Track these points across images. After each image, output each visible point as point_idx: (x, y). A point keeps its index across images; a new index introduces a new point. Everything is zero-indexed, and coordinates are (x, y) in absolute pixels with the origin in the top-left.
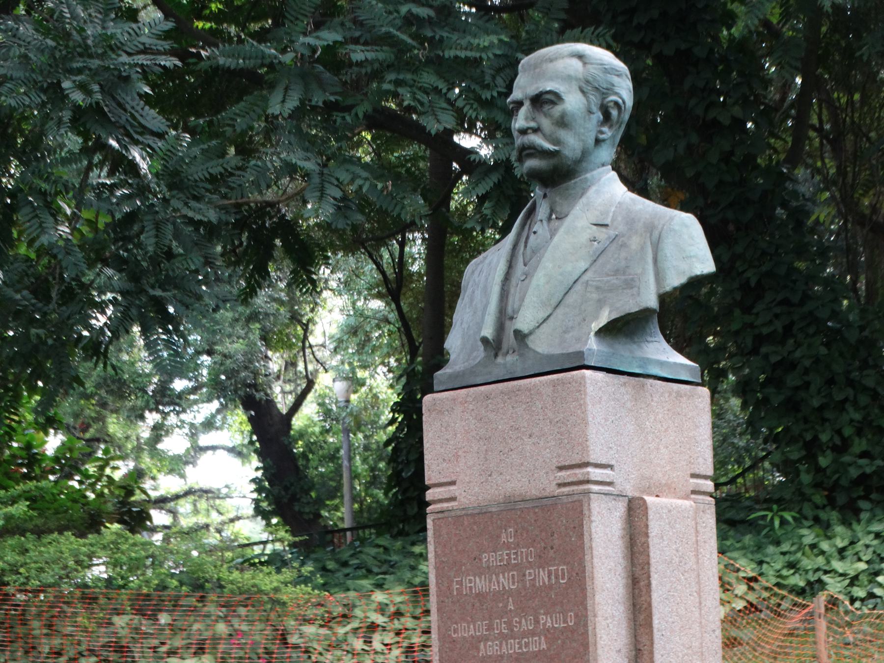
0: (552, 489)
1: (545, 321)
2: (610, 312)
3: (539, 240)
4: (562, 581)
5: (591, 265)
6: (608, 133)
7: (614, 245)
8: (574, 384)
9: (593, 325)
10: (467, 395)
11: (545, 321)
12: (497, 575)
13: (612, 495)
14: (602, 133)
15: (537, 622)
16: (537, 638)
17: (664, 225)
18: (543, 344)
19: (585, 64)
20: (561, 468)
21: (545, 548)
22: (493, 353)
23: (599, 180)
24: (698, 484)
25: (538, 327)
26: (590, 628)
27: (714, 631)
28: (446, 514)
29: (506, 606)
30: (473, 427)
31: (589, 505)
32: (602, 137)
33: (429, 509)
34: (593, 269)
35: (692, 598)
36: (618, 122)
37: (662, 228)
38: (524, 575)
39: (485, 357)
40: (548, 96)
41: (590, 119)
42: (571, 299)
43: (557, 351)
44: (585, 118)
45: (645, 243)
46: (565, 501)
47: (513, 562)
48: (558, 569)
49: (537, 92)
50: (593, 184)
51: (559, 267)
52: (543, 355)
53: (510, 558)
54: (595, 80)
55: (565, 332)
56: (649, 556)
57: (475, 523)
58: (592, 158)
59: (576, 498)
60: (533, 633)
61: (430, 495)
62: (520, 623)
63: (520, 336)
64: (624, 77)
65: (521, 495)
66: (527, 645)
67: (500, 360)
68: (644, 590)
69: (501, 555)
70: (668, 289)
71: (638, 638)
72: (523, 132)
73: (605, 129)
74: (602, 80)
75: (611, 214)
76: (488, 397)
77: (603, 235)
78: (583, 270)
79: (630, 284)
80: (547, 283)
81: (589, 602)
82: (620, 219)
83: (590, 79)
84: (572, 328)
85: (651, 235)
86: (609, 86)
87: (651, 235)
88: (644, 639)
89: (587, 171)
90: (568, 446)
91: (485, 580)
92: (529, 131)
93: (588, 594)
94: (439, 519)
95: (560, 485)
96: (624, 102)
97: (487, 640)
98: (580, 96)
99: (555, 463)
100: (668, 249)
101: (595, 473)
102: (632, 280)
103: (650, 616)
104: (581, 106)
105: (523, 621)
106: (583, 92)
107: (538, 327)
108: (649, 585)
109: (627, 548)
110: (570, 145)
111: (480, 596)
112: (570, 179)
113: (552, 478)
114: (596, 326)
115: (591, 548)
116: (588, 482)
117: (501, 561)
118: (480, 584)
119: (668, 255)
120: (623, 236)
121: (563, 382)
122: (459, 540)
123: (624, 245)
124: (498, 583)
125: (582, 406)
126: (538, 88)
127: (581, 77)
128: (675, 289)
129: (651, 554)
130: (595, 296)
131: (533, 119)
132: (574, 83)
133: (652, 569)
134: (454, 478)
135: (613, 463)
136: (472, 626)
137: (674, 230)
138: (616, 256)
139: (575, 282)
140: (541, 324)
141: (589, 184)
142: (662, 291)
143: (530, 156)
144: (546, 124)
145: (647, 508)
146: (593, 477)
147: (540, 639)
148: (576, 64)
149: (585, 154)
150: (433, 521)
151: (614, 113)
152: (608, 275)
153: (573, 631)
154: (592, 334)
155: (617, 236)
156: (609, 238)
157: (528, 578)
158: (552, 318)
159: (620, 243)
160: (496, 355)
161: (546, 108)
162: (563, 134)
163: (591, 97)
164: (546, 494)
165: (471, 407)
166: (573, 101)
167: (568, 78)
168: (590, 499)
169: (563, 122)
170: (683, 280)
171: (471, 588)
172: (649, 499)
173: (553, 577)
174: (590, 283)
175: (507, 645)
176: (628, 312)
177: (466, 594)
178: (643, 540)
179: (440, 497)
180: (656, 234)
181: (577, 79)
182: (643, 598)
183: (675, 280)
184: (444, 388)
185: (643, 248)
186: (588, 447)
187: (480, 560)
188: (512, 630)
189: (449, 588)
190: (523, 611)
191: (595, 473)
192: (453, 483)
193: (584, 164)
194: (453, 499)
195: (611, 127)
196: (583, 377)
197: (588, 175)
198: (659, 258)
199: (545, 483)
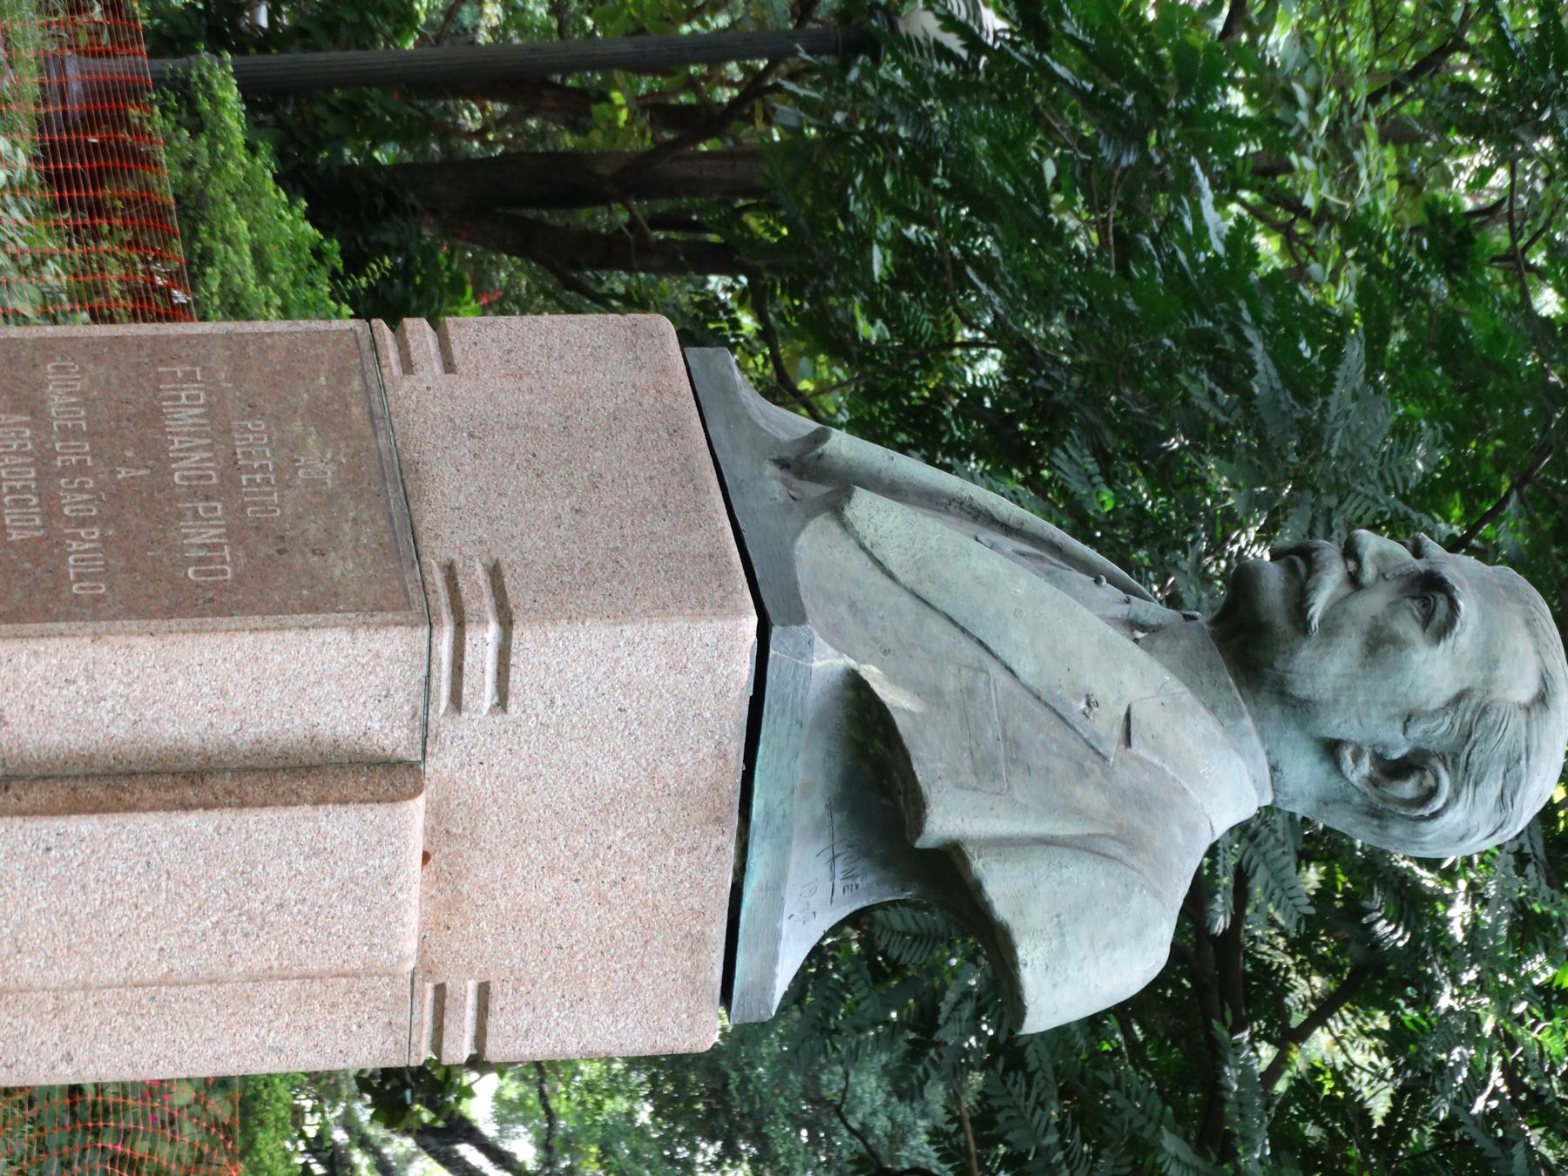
0: (436, 554)
1: (879, 564)
2: (910, 713)
3: (1079, 587)
4: (190, 572)
5: (1025, 686)
6: (1359, 771)
7: (1082, 750)
8: (721, 593)
9: (874, 669)
10: (677, 395)
11: (879, 564)
12: (209, 448)
13: (427, 706)
14: (1356, 757)
15: (82, 523)
16: (38, 522)
17: (1140, 872)
18: (816, 550)
19: (1527, 709)
20: (495, 572)
21: (282, 538)
22: (788, 454)
23: (1237, 751)
24: (463, 1006)
25: (863, 547)
26: (62, 626)
27: (68, 1058)
28: (368, 354)
29: (125, 463)
30: (597, 403)
31: (397, 624)
32: (1347, 755)
33: (380, 324)
34: (1018, 691)
35: (154, 957)
36: (1385, 800)
37: (1133, 868)
38: (207, 498)
39: (778, 442)
40: (1442, 606)
41: (1391, 718)
42: (936, 626)
43: (803, 574)
44: (1393, 703)
45: (1092, 820)
46: (407, 577)
47: (244, 478)
48: (224, 562)
49: (1450, 580)
50: (1228, 731)
51: (1017, 613)
52: (792, 547)
53: (255, 471)
54: (1490, 730)
55: (852, 605)
56: (264, 805)
58: (1292, 733)
59: (417, 597)
60: (51, 513)
61: (418, 328)
62: (81, 490)
63: (835, 508)
64: (1497, 819)
66: (22, 503)
67: (771, 470)
68: (171, 796)
70: (978, 866)
71: (40, 783)
72: (1350, 551)
73: (1366, 767)
74: (1489, 752)
75: (1156, 761)
76: (673, 432)
77: (1106, 726)
78: (1014, 667)
79: (984, 774)
80: (977, 579)
81: (134, 625)
82: (1146, 777)
83: (1491, 719)
84: (865, 624)
85: (1113, 838)
86: (1474, 771)
87: (1113, 838)
88: (37, 795)
89: (1258, 719)
90: (555, 583)
91: (194, 425)
92: (1352, 565)
93: (154, 622)
94: (357, 341)
96: (1435, 815)
98: (1448, 690)
99: (508, 557)
100: (1081, 875)
101: (484, 639)
102: (996, 776)
103: (98, 808)
104: (1423, 694)
105: (86, 497)
106: (1459, 698)
107: (863, 547)
108: (186, 807)
109: (285, 755)
110: (1325, 668)
112: (1235, 676)
113: (467, 550)
114: (872, 674)
115: (282, 628)
116: (460, 625)
117: (248, 455)
119: (1066, 873)
120: (1105, 774)
121: (723, 573)
123: (1082, 773)
124: (189, 450)
125: (662, 609)
126: (1461, 585)
127: (1496, 694)
128: (978, 886)
129: (267, 814)
130: (950, 684)
131: (1382, 575)
132: (1480, 675)
133: (228, 816)
135: (513, 707)
136: (73, 400)
137: (1129, 895)
138: (1055, 748)
139: (981, 643)
140: (870, 555)
141: (1228, 722)
142: (969, 850)
144: (1373, 603)
145: (393, 801)
146: (472, 635)
147: (36, 528)
148: (1525, 691)
149: (1298, 708)
151: (1408, 788)
152: (1004, 722)
154: (853, 663)
155: (1105, 758)
156: (1099, 740)
157: (201, 506)
158: (888, 582)
159: (1088, 764)
160: (783, 464)
161: (1415, 605)
162: (1350, 645)
163: (1447, 721)
164: (424, 543)
166: (1433, 671)
167: (1489, 661)
168: (414, 626)
169: (1379, 643)
170: (1002, 909)
171: (178, 398)
172: (416, 810)
174: (983, 677)
175: (28, 465)
176: (913, 754)
177: (159, 390)
178: (307, 793)
179: (412, 344)
180: (1118, 850)
181: (1488, 682)
182: (148, 793)
183: (1002, 887)
184: (691, 365)
185: (1079, 813)
186: (553, 620)
187: (250, 416)
188: (60, 475)
189: (176, 358)
190: (111, 496)
191: (484, 639)
192: (449, 366)
193: (1275, 711)
194: (408, 366)
195: (1373, 782)
196: (738, 612)
197: (1248, 722)
198: (1057, 850)
199: (454, 531)
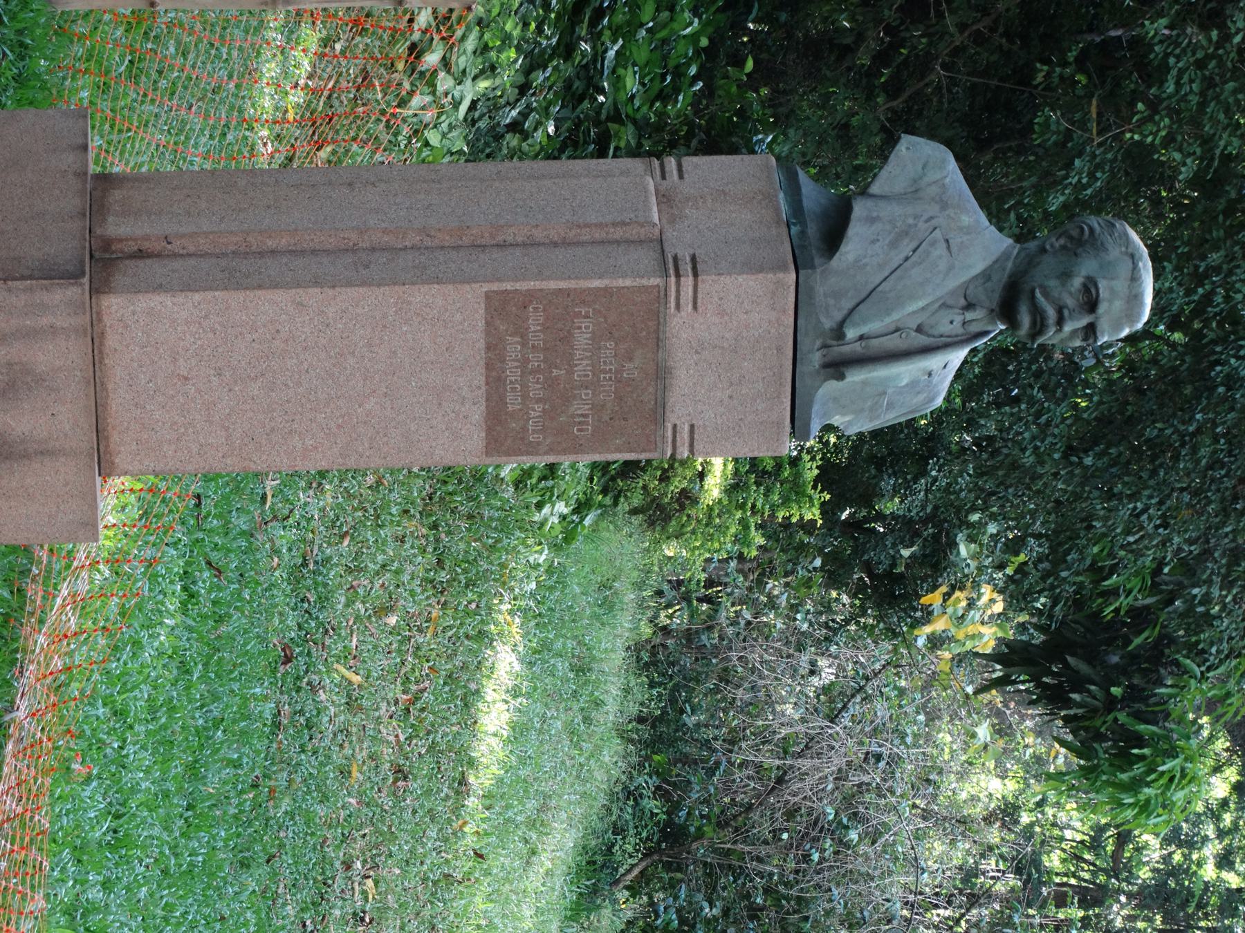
0: (672, 419)
20: (692, 426)
38: (587, 388)
53: (605, 372)
57: (649, 333)
59: (659, 445)
60: (525, 397)
62: (537, 383)
65: (671, 385)
69: (611, 363)
95: (675, 426)
97: (524, 345)
111: (567, 339)
118: (582, 339)
122: (632, 315)
134: (700, 310)
143: (1034, 323)
150: (658, 285)
153: (522, 439)
164: (668, 414)
165: (773, 331)
171: (580, 328)
173: (582, 419)
192: (695, 307)
